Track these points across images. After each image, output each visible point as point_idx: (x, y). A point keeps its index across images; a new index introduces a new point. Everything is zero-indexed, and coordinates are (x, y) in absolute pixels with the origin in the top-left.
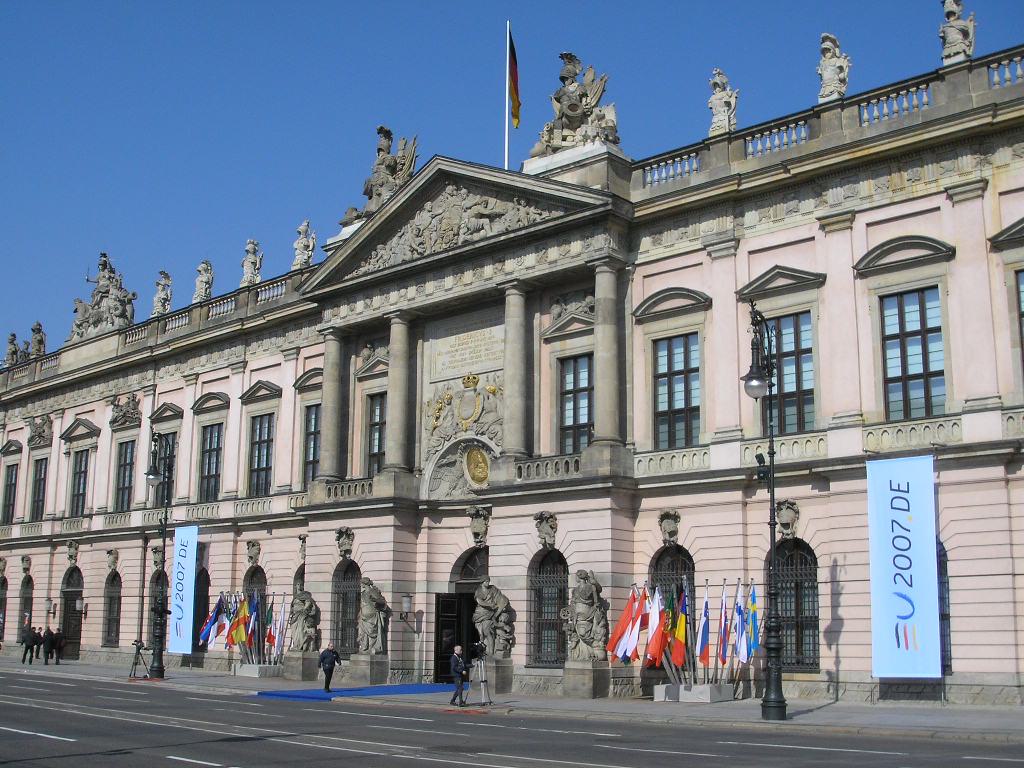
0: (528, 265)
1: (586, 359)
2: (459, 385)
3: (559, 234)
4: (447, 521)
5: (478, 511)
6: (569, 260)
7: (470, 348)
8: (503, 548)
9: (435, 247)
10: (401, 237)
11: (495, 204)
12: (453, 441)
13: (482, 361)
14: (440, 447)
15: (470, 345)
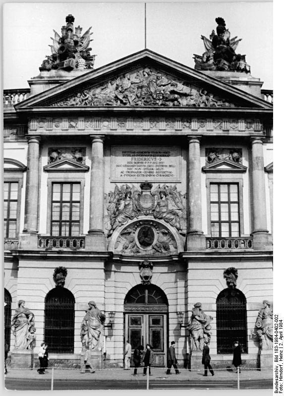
0: (211, 129)
1: (236, 186)
2: (137, 187)
3: (234, 117)
4: (124, 268)
5: (150, 264)
6: (237, 132)
7: (145, 166)
8: (94, 283)
9: (133, 101)
10: (103, 89)
11: (181, 87)
12: (135, 220)
13: (154, 176)
14: (124, 223)
15: (144, 164)
